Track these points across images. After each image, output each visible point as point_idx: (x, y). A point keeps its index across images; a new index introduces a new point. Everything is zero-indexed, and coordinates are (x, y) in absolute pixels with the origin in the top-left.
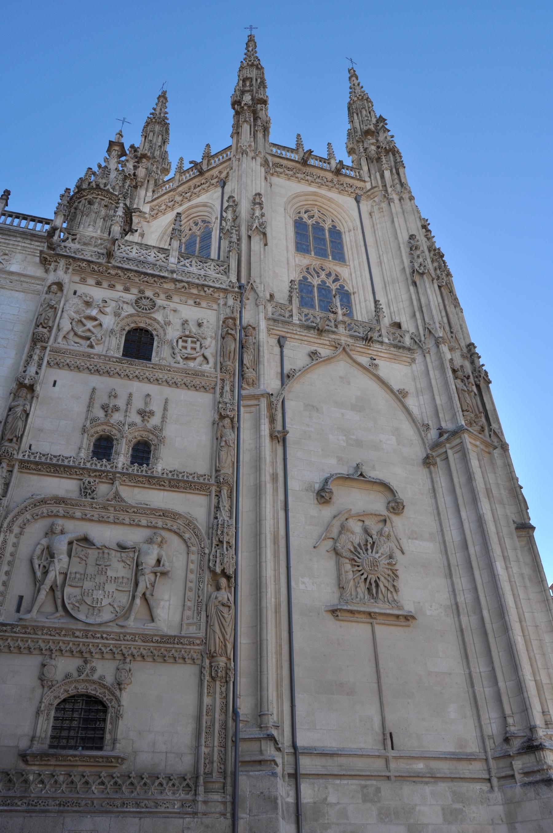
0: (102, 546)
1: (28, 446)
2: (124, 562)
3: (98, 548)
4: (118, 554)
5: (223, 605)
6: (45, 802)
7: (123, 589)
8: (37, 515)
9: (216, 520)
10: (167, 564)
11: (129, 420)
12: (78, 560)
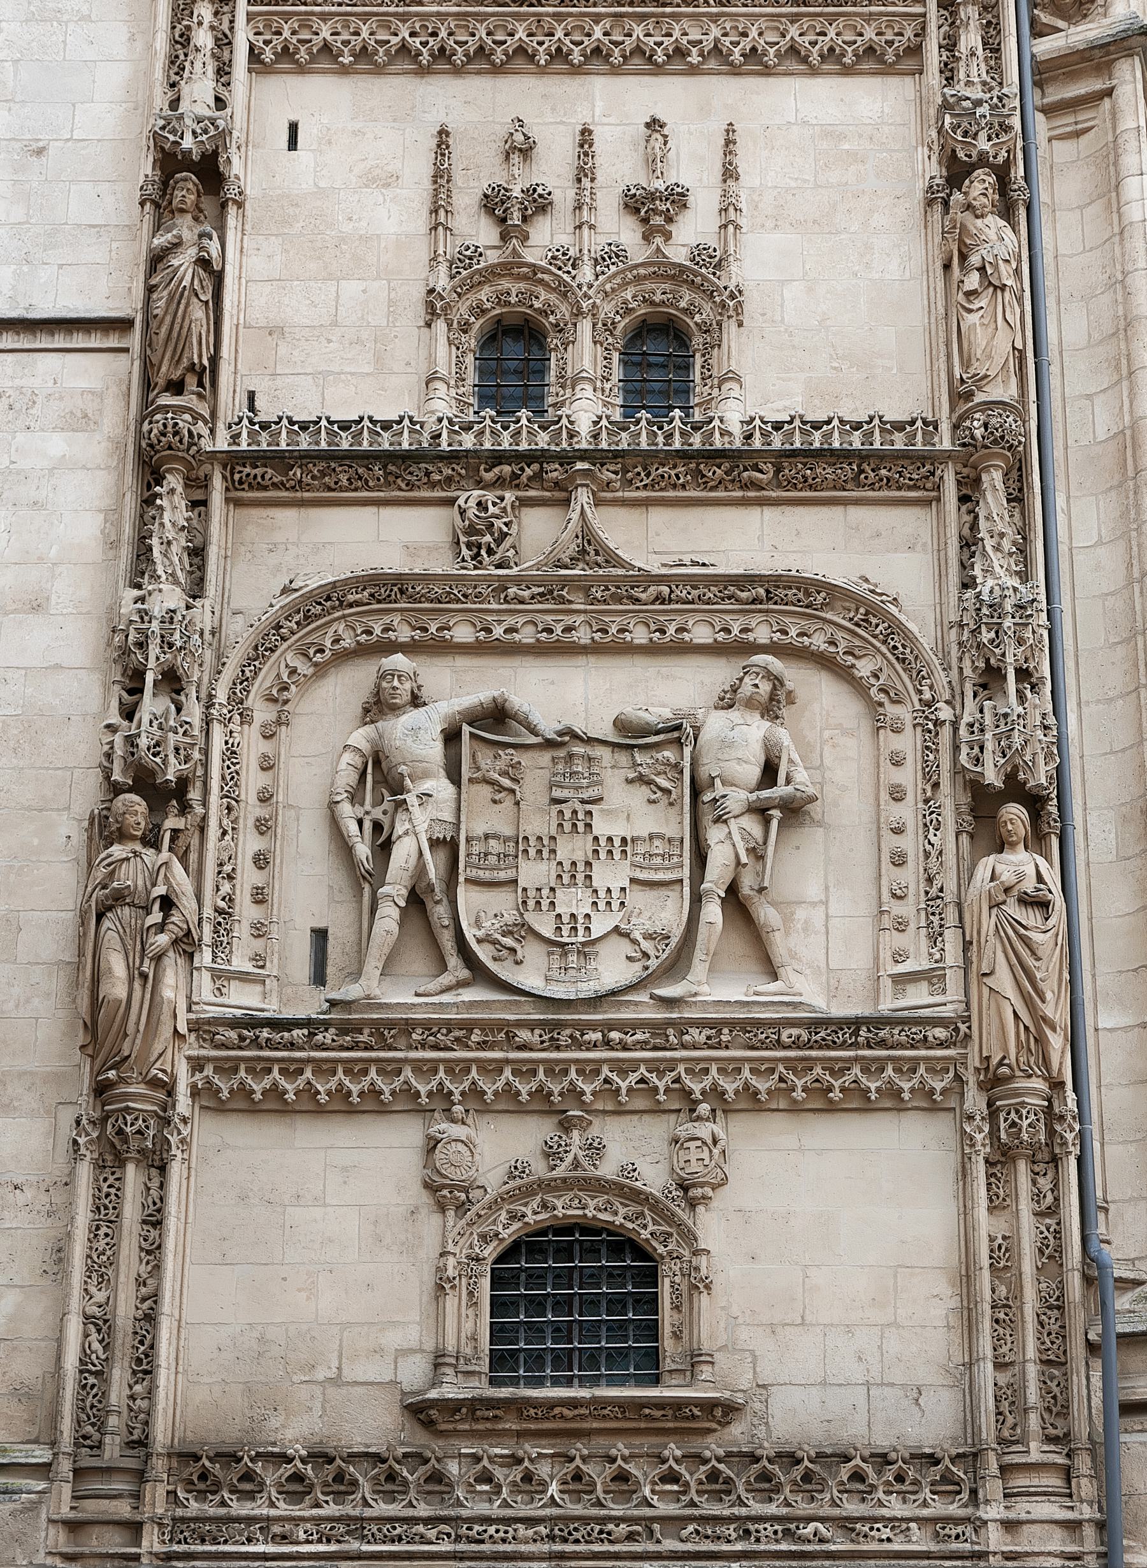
0: (561, 734)
1: (242, 399)
2: (649, 783)
3: (549, 744)
4: (623, 758)
5: (1026, 901)
6: (506, 1532)
7: (660, 876)
8: (322, 651)
9: (970, 594)
10: (801, 776)
11: (595, 243)
12: (486, 791)
